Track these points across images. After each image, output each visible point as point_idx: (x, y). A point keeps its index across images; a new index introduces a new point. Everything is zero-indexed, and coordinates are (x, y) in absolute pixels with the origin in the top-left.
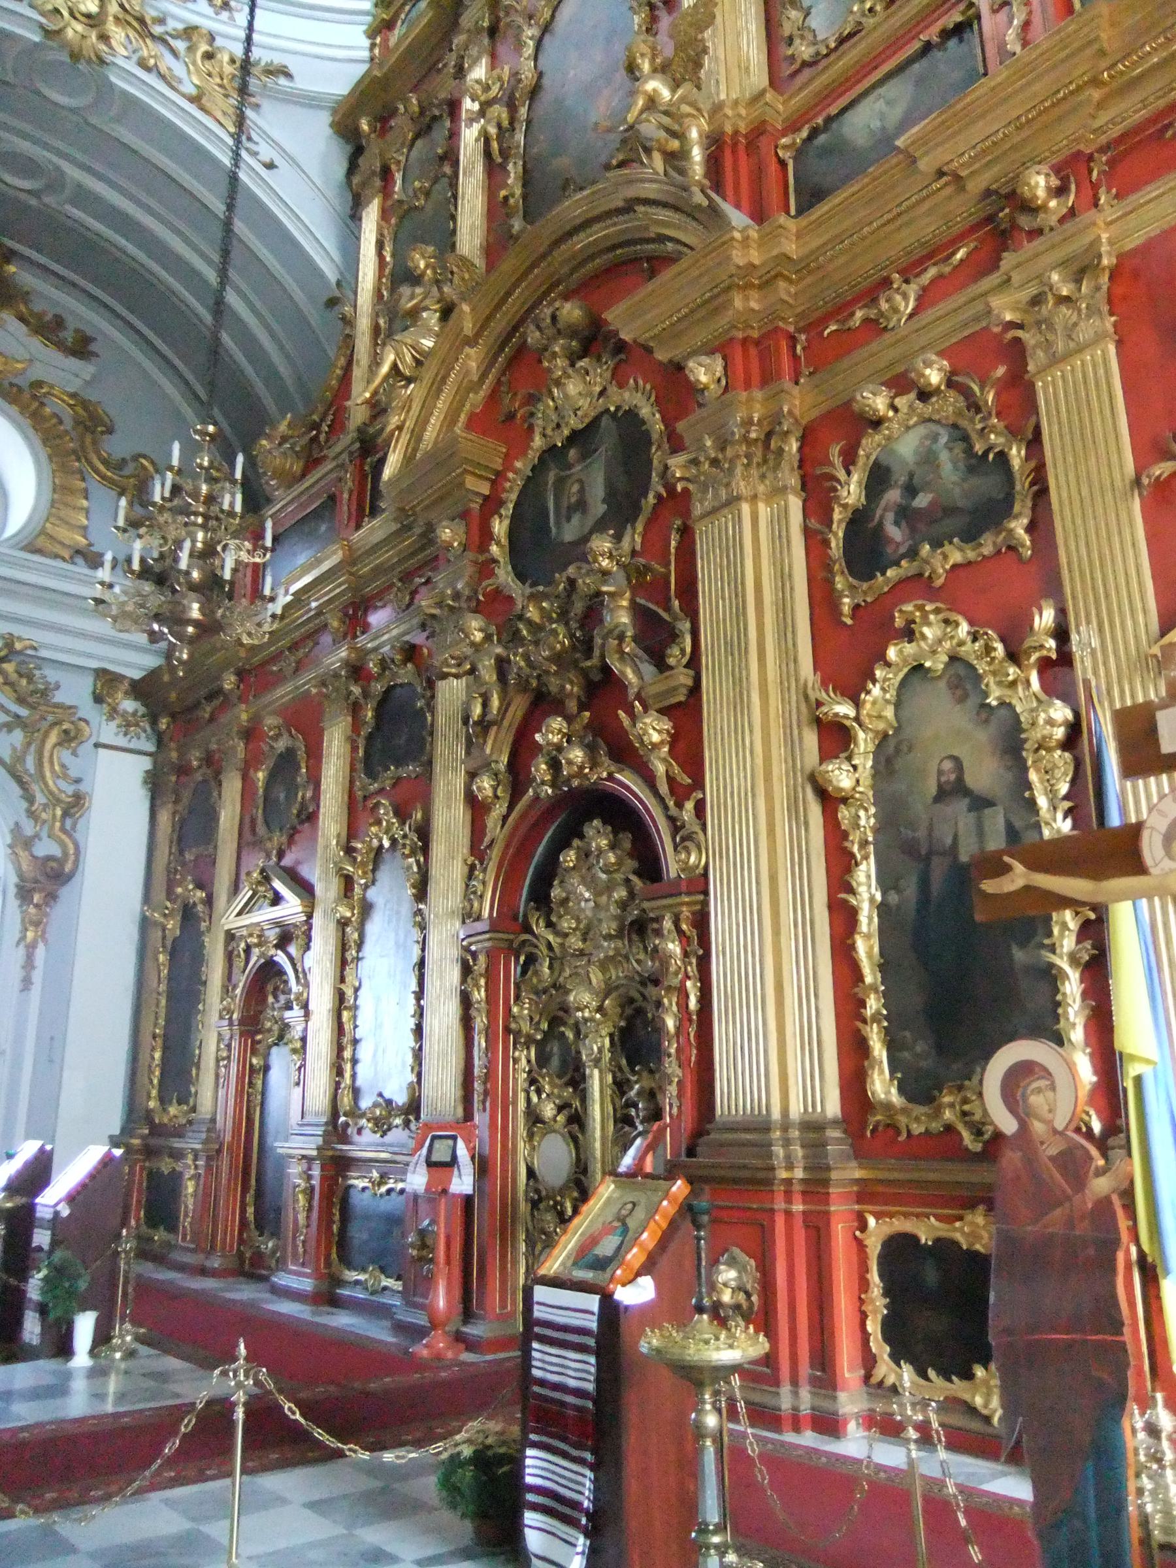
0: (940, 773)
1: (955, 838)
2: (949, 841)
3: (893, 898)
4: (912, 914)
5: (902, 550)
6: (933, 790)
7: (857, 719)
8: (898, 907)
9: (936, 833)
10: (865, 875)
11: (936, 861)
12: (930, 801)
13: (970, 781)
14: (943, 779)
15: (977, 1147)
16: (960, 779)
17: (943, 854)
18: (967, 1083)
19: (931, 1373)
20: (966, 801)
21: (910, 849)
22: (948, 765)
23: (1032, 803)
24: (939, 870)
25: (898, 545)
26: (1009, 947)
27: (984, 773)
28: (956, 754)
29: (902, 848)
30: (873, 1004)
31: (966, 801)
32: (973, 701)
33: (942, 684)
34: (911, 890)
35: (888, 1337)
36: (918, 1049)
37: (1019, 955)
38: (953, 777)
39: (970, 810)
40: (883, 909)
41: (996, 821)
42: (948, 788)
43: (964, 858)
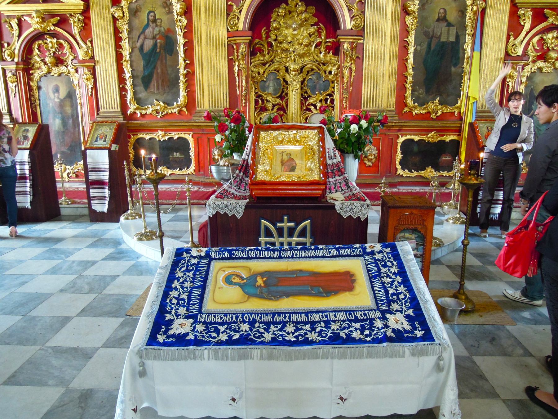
0: (439, 13)
2: (439, 34)
3: (419, 48)
4: (424, 54)
6: (437, 18)
9: (435, 31)
10: (411, 39)
11: (434, 39)
13: (448, 17)
14: (440, 15)
15: (435, 117)
16: (445, 16)
19: (413, 171)
20: (446, 24)
21: (426, 34)
22: (442, 11)
23: (465, 28)
24: (434, 42)
26: (451, 68)
27: (452, 16)
29: (425, 34)
30: (410, 79)
31: (446, 24)
34: (425, 45)
35: (401, 164)
36: (420, 92)
37: (453, 69)
38: (443, 15)
40: (415, 51)
41: (453, 31)
42: (441, 18)
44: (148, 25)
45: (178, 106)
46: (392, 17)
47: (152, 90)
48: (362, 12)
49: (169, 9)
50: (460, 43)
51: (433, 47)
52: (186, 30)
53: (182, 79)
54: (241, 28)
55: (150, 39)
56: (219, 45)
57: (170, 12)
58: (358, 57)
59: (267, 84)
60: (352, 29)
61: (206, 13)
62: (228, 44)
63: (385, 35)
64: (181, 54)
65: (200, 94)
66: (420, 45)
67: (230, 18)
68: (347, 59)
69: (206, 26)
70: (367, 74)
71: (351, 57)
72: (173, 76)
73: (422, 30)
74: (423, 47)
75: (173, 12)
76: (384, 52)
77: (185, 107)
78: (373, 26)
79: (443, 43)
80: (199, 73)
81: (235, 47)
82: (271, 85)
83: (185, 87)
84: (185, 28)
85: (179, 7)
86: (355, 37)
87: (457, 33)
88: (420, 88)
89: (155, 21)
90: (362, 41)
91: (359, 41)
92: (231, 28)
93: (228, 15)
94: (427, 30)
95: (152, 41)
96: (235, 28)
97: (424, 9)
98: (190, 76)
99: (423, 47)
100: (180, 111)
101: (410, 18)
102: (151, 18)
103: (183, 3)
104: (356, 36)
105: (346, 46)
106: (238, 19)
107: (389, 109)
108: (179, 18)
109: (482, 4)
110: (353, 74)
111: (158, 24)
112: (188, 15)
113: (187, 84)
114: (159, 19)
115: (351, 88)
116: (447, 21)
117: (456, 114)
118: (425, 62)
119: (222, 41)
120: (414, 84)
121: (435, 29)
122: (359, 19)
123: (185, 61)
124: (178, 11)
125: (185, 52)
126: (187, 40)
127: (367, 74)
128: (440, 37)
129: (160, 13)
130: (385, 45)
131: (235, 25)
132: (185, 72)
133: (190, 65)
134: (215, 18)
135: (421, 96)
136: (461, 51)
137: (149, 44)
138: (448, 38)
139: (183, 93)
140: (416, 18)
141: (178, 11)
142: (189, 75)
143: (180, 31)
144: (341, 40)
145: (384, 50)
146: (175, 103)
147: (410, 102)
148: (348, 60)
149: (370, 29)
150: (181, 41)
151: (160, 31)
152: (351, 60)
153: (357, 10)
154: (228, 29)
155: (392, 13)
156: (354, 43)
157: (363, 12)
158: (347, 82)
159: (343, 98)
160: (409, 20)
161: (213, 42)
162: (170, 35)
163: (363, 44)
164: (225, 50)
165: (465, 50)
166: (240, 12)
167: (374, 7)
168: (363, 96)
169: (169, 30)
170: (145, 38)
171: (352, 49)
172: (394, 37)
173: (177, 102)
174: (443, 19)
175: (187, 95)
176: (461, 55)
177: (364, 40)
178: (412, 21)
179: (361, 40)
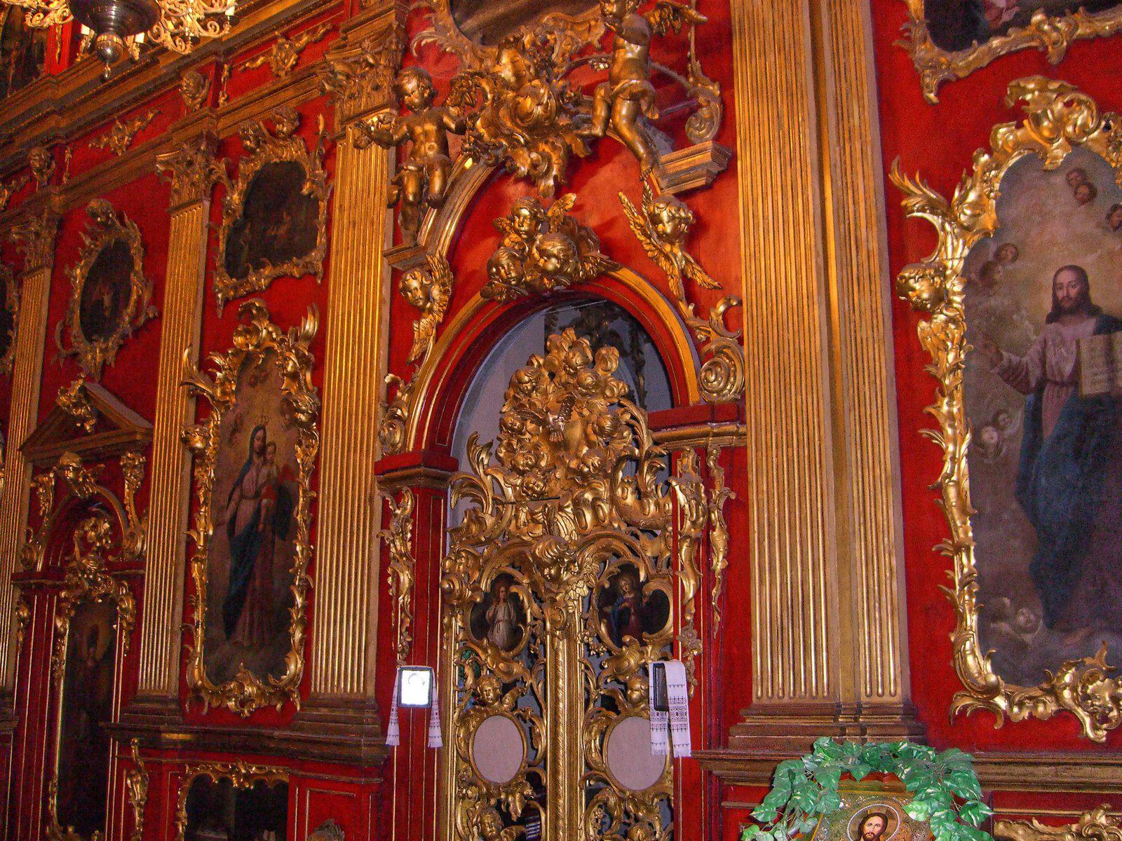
0: (1056, 286)
2: (1068, 368)
3: (990, 436)
5: (1006, 17)
6: (1048, 306)
8: (998, 448)
11: (1047, 392)
12: (1042, 319)
14: (1060, 294)
16: (1084, 295)
17: (1062, 384)
18: (1088, 661)
20: (1090, 325)
21: (1015, 376)
22: (1066, 277)
25: (1001, 11)
28: (1078, 262)
29: (1007, 376)
31: (1090, 325)
33: (1059, 180)
34: (1016, 423)
36: (1021, 619)
38: (1073, 292)
39: (1098, 331)
42: (1066, 305)
43: (1088, 389)
44: (250, 461)
47: (239, 639)
51: (1050, 429)
55: (250, 499)
59: (489, 613)
66: (995, 423)
73: (993, 365)
74: (1009, 431)
79: (1098, 400)
82: (500, 615)
88: (1018, 604)
89: (262, 451)
95: (252, 502)
99: (1009, 431)
102: (257, 443)
110: (719, 563)
111: (268, 457)
114: (270, 444)
116: (1094, 311)
118: (1025, 488)
120: (990, 591)
121: (1050, 354)
128: (1075, 379)
129: (275, 433)
135: (1028, 638)
137: (247, 508)
138: (1111, 380)
147: (976, 664)
151: (269, 475)
170: (242, 497)
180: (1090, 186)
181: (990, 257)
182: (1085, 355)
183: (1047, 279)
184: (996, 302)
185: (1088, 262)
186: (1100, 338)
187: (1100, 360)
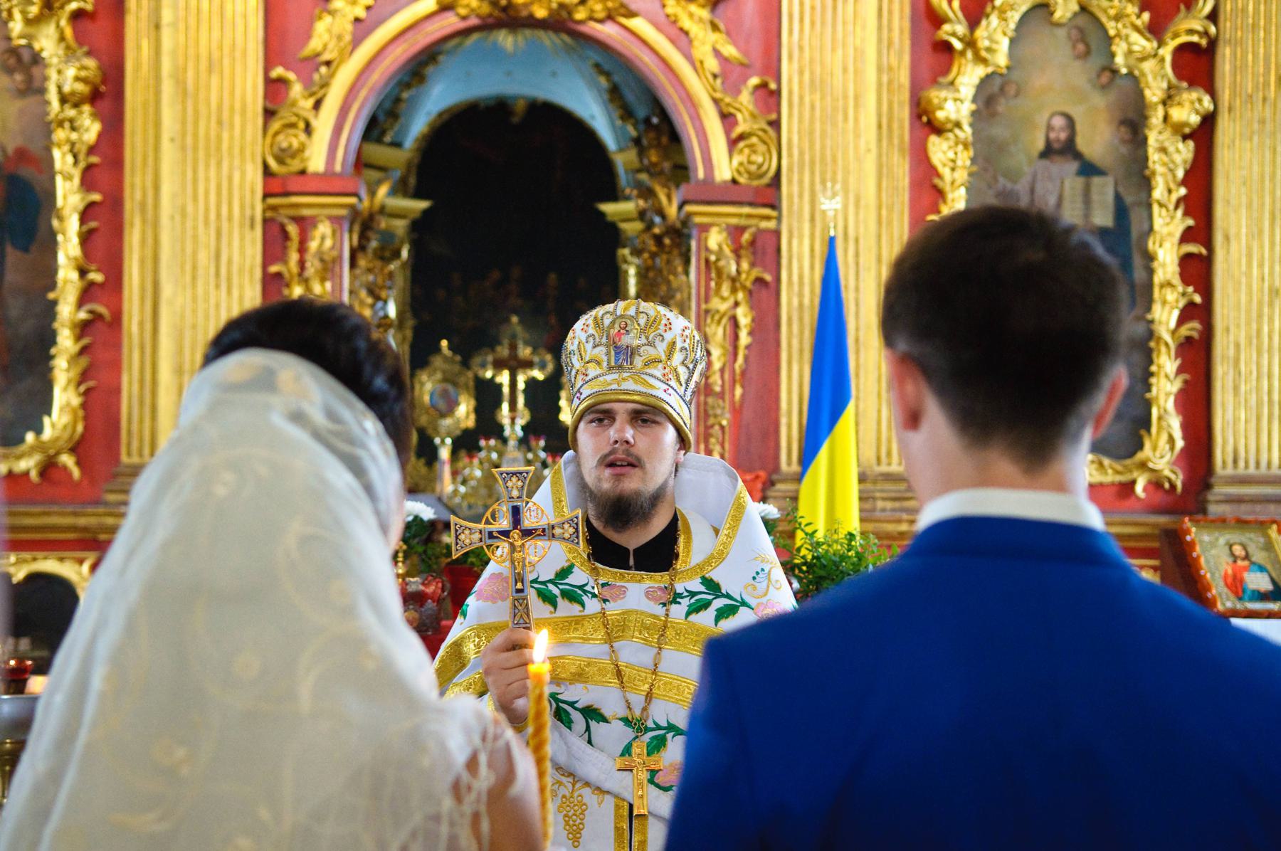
0: (1050, 128)
1: (1060, 199)
2: (1052, 200)
6: (1040, 145)
7: (970, 43)
9: (1039, 189)
13: (1082, 144)
20: (1073, 166)
22: (1059, 122)
23: (1146, 183)
27: (1097, 140)
31: (1073, 166)
32: (1096, 62)
33: (1061, 33)
38: (1063, 136)
41: (1104, 190)
42: (1056, 146)
45: (40, 447)
46: (879, 140)
48: (771, 123)
49: (29, 79)
50: (1134, 234)
52: (94, 159)
53: (66, 342)
54: (316, 161)
56: (230, 219)
57: (33, 88)
58: (759, 281)
60: (734, 181)
61: (184, 102)
62: (266, 221)
63: (857, 205)
64: (69, 247)
65: (141, 403)
67: (276, 125)
68: (719, 285)
69: (183, 148)
70: (795, 342)
71: (733, 280)
72: (27, 327)
73: (990, 187)
75: (42, 91)
76: (857, 264)
77: (73, 450)
78: (812, 173)
80: (141, 324)
81: (292, 229)
83: (75, 373)
84: (92, 150)
85: (71, 72)
86: (746, 210)
87: (1118, 198)
90: (771, 225)
91: (765, 225)
92: (280, 161)
93: (269, 114)
94: (1009, 185)
96: (295, 165)
97: (994, 115)
98: (101, 332)
100: (49, 468)
101: (945, 145)
103: (91, 63)
104: (751, 204)
105: (715, 239)
106: (308, 129)
107: (884, 468)
108: (71, 113)
109: (1200, 100)
110: (744, 339)
112: (105, 104)
113: (84, 362)
115: (738, 391)
116: (1078, 156)
117: (1139, 489)
119: (242, 207)
122: (762, 148)
123: (83, 272)
124: (67, 89)
125: (86, 239)
126: (96, 197)
127: (795, 342)
130: (857, 240)
131: (302, 149)
132: (83, 315)
133: (104, 289)
134: (220, 123)
136: (1137, 261)
139: (65, 396)
140: (966, 146)
141: (67, 89)
142: (99, 325)
143: (70, 159)
144: (697, 220)
145: (857, 255)
146: (30, 437)
148: (725, 290)
149: (801, 182)
150: (69, 196)
152: (734, 290)
153: (753, 116)
154: (266, 167)
155: (880, 126)
156: (740, 230)
157: (776, 125)
158: (722, 371)
159: (708, 428)
160: (939, 150)
161: (207, 210)
162: (26, 172)
163: (777, 233)
164: (253, 242)
165: (1149, 258)
166: (317, 105)
167: (813, 107)
168: (783, 421)
169: (22, 155)
171: (737, 252)
172: (890, 210)
173: (39, 430)
174: (1063, 149)
175: (84, 406)
176: (1139, 274)
177: (779, 219)
178: (951, 155)
179: (768, 218)
180: (1087, 46)
181: (996, 89)
182: (1067, 192)
183: (1042, 119)
184: (998, 131)
185: (1077, 112)
186: (1080, 181)
187: (1079, 199)
